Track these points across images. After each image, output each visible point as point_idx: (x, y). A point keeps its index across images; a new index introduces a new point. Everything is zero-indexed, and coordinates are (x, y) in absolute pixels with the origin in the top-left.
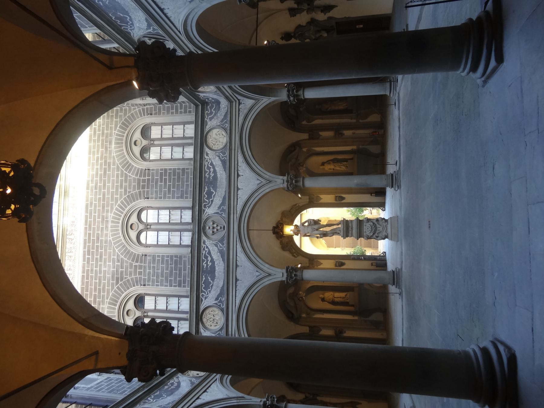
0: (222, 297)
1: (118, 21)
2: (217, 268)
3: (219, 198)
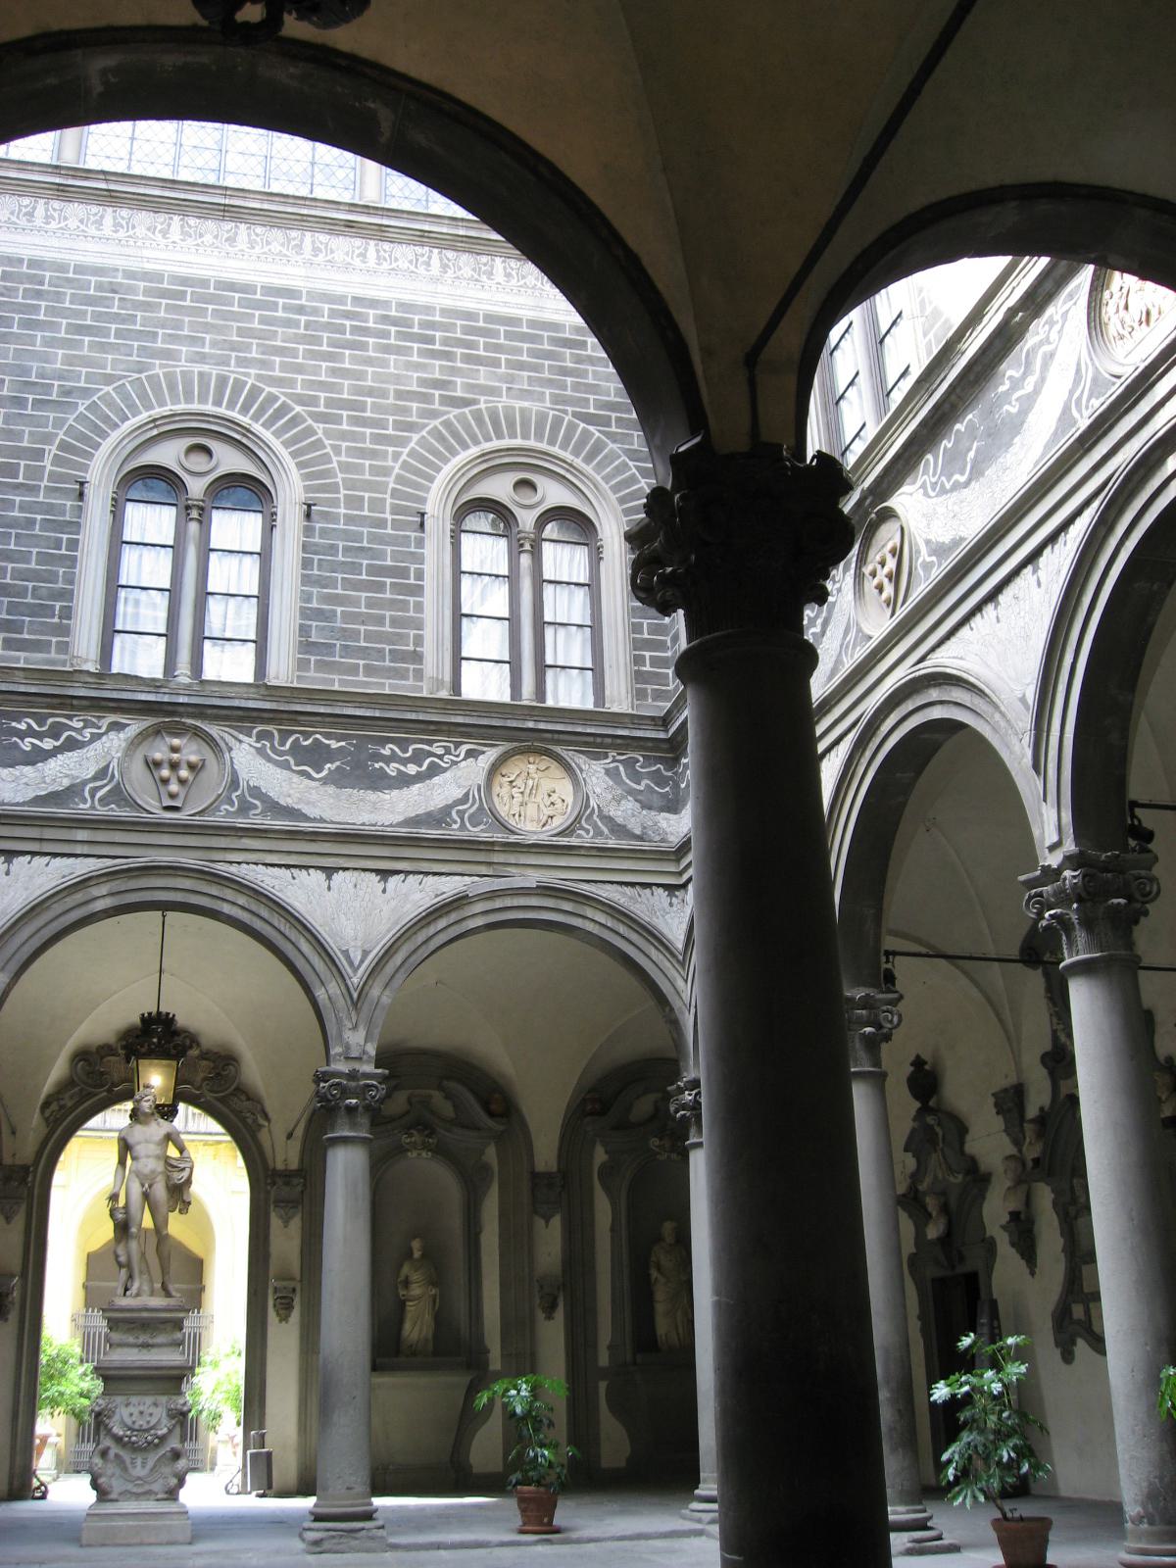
1: (949, 442)
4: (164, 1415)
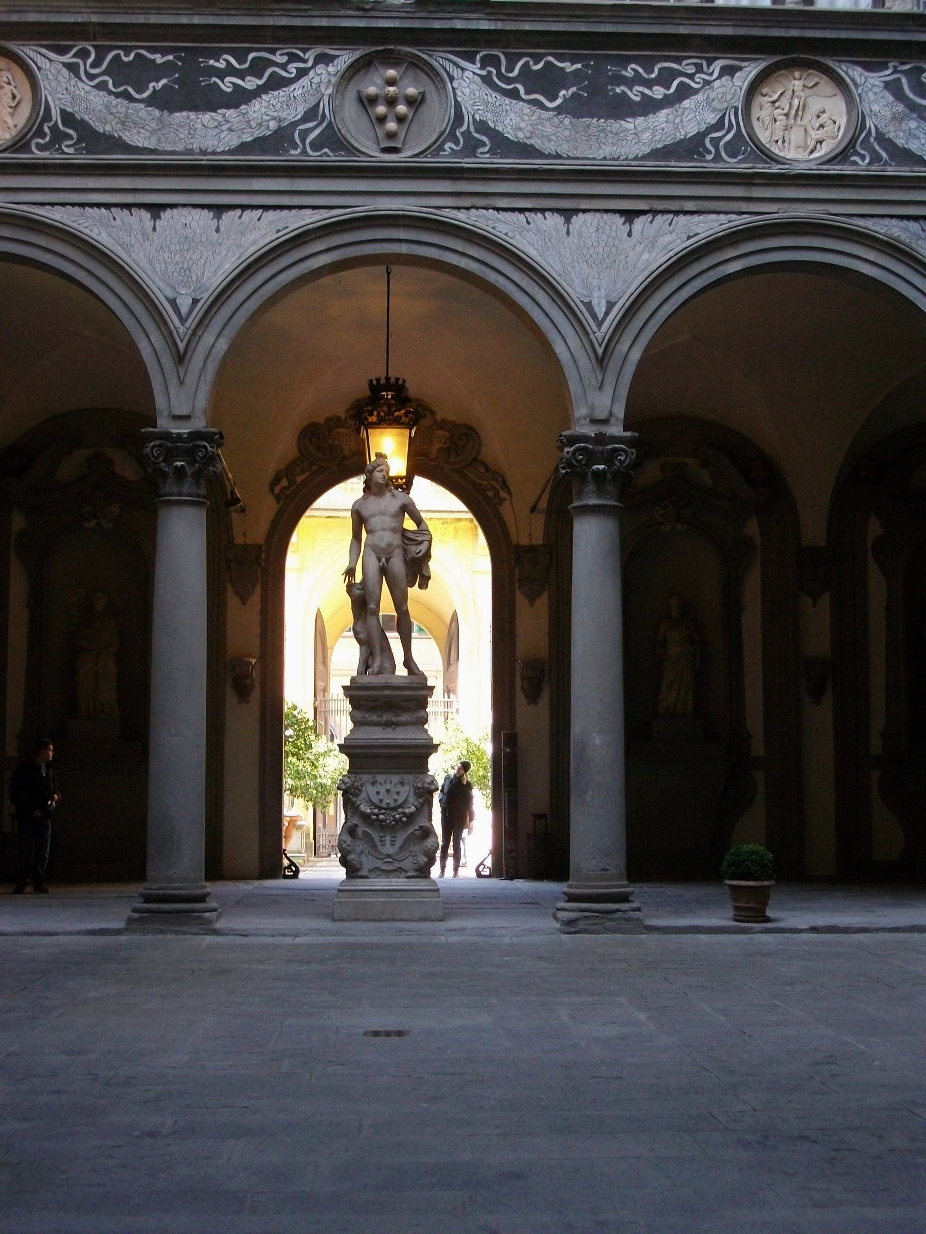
0: (79, 141)
2: (207, 117)
3: (530, 128)
4: (411, 792)
